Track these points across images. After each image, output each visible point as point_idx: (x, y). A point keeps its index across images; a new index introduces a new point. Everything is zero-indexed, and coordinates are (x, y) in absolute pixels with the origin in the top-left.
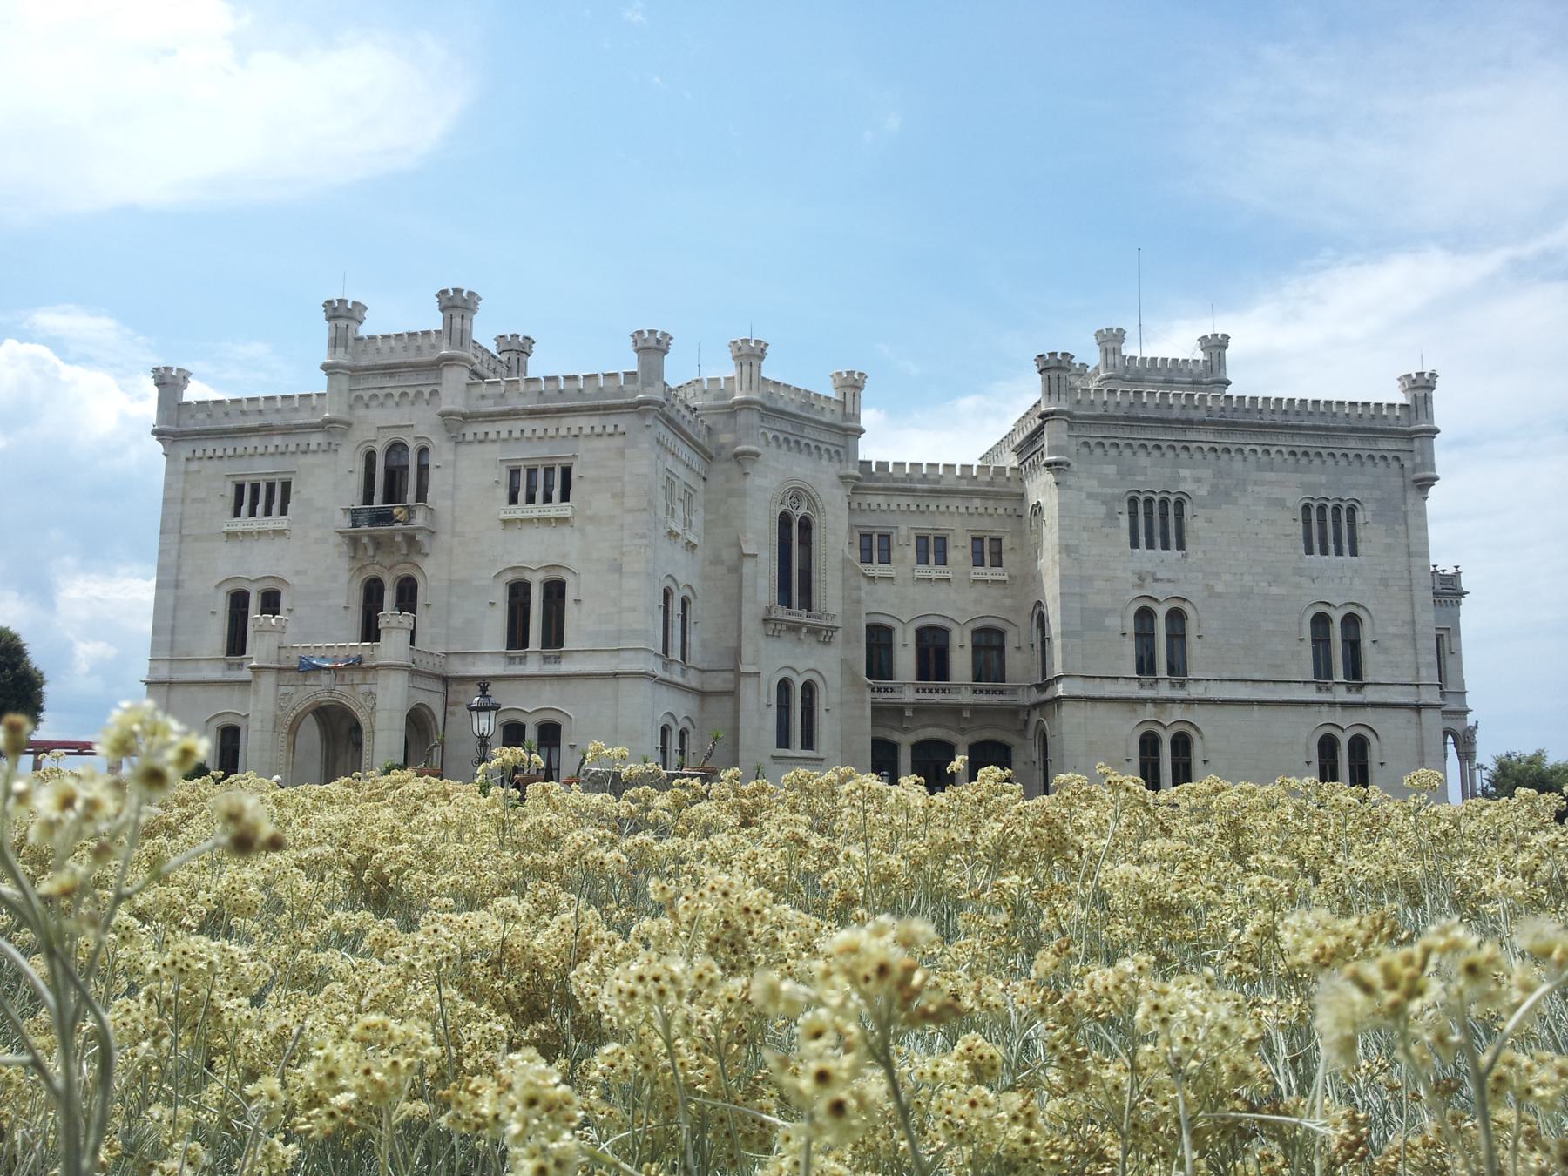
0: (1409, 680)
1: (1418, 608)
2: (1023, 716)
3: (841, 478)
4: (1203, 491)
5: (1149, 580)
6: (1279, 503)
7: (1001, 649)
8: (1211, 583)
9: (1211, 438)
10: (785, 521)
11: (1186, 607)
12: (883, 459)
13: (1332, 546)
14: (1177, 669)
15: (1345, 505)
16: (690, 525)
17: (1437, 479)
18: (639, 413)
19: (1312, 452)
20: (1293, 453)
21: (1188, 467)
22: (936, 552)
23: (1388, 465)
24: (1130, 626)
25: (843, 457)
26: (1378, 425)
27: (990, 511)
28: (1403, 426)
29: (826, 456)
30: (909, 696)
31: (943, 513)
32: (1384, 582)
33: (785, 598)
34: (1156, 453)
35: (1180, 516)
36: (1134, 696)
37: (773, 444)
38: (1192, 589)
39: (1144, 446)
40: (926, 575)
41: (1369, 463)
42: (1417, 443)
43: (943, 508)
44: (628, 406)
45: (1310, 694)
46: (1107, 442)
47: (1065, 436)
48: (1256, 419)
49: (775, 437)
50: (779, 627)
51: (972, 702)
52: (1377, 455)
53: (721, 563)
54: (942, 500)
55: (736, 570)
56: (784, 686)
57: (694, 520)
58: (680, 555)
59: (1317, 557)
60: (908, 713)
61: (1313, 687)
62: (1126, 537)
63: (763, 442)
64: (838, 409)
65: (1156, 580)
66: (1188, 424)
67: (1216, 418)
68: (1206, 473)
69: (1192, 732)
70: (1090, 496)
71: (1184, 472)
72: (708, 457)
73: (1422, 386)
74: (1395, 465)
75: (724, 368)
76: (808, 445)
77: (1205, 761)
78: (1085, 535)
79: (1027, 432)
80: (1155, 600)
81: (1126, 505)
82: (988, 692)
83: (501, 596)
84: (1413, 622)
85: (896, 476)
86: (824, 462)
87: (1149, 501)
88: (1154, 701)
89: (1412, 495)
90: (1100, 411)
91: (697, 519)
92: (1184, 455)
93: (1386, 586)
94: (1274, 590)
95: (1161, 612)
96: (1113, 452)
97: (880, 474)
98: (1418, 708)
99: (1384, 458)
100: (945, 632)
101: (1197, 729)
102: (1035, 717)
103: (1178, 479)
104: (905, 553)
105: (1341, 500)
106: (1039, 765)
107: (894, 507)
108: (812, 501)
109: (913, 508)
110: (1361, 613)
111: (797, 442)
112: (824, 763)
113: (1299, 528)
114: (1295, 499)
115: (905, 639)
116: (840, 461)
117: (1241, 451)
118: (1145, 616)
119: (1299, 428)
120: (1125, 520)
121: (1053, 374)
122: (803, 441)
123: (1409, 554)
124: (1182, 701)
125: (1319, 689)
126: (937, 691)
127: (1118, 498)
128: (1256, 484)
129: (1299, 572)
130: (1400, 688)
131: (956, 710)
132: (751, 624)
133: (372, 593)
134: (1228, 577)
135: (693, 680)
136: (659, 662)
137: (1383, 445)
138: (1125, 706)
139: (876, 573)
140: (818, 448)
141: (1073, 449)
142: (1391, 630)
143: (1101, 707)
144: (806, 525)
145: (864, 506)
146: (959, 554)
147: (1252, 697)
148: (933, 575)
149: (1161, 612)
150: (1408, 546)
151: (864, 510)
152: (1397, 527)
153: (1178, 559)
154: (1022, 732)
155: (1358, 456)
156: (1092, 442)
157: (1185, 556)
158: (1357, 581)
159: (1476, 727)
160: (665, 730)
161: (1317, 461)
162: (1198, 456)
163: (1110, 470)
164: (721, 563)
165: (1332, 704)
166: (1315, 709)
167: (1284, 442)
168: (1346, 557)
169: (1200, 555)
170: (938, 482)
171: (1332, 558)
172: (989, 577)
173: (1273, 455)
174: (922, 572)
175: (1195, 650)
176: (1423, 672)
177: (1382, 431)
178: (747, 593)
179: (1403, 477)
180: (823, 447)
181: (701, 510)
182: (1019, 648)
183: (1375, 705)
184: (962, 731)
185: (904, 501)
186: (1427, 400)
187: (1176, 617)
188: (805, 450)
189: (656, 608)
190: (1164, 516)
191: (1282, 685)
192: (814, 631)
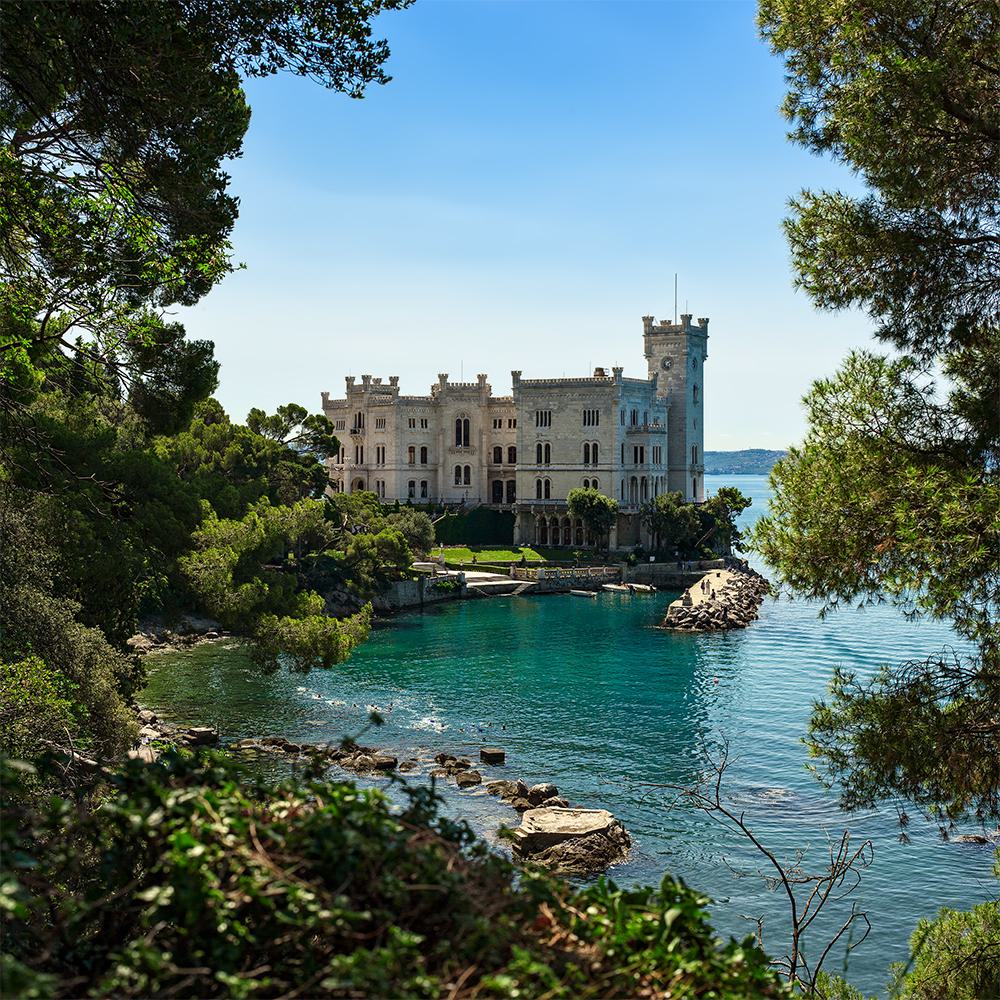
10: (459, 421)
14: (548, 461)
24: (535, 449)
32: (605, 433)
45: (582, 467)
56: (458, 469)
62: (535, 423)
83: (376, 450)
98: (611, 471)
114: (581, 409)
118: (539, 446)
120: (535, 418)
129: (580, 431)
133: (357, 447)
135: (429, 467)
144: (467, 422)
163: (531, 404)
187: (548, 447)
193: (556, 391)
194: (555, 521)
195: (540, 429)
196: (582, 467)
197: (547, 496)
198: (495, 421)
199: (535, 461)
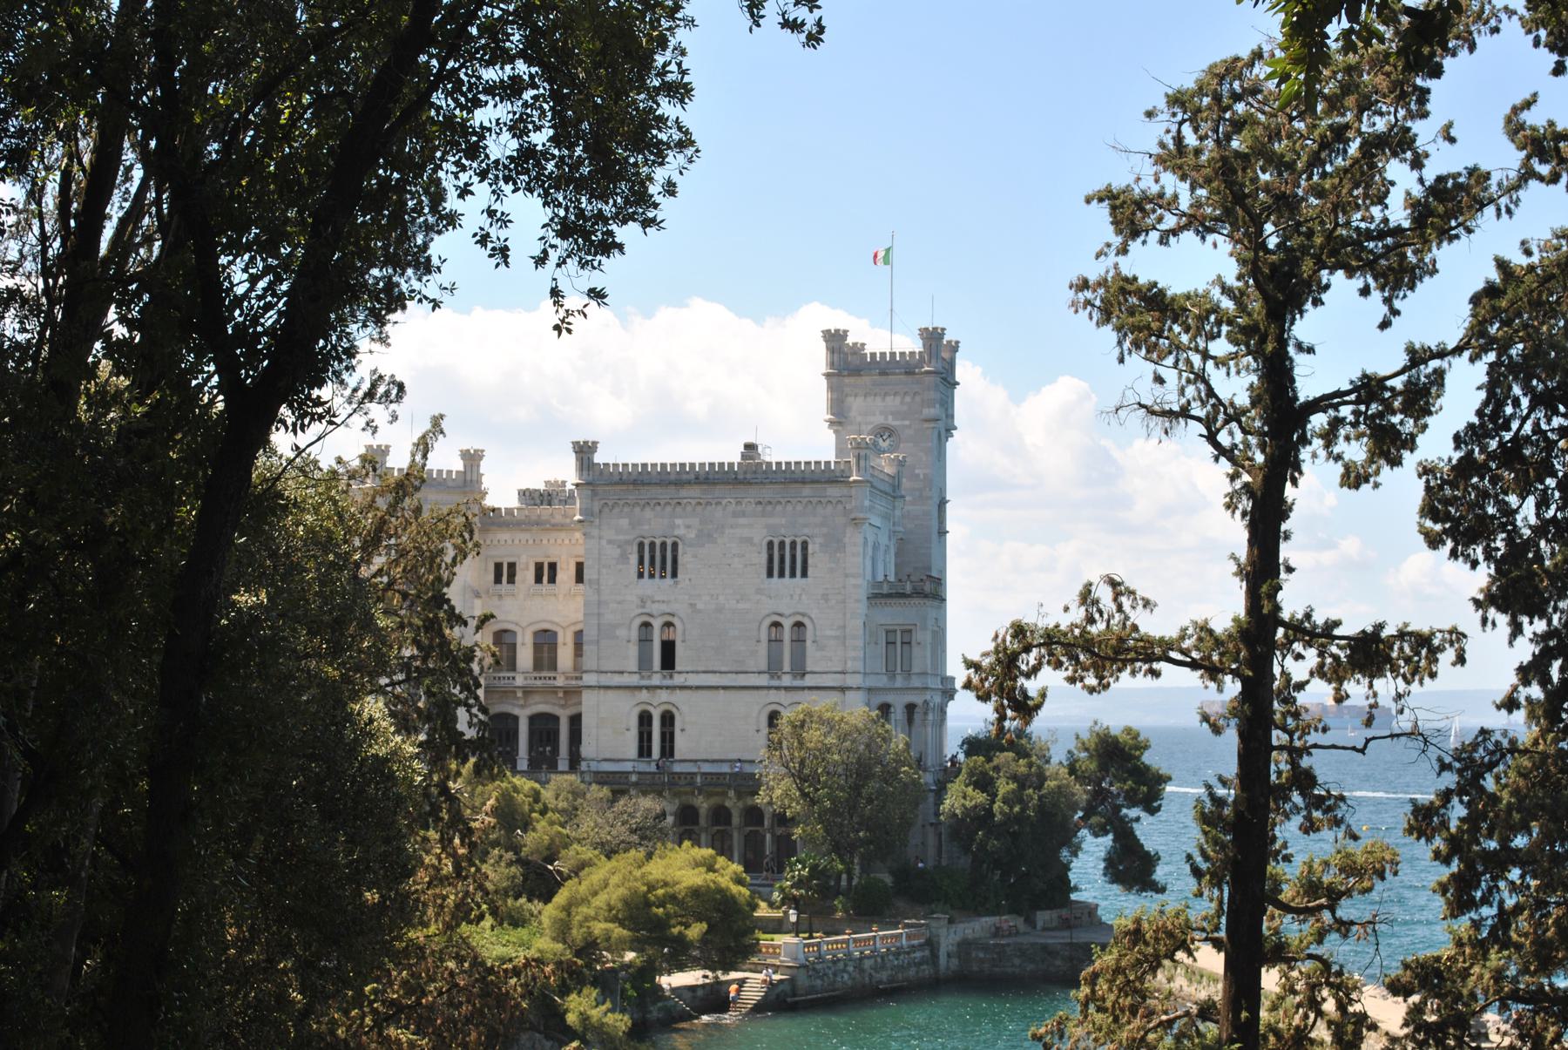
0: (840, 669)
1: (848, 616)
4: (693, 536)
6: (749, 541)
11: (676, 621)
14: (668, 661)
19: (773, 501)
20: (760, 503)
21: (681, 517)
24: (634, 634)
32: (825, 597)
34: (658, 508)
38: (680, 608)
45: (763, 680)
60: (520, 694)
68: (695, 522)
69: (674, 710)
70: (610, 542)
71: (678, 521)
77: (682, 730)
81: (635, 548)
87: (652, 545)
88: (647, 688)
90: (617, 478)
93: (827, 600)
94: (740, 606)
97: (508, 518)
98: (843, 689)
100: (555, 633)
103: (673, 526)
104: (526, 575)
107: (517, 542)
109: (531, 542)
110: (806, 621)
114: (760, 536)
120: (634, 559)
124: (667, 688)
125: (772, 677)
127: (628, 543)
128: (732, 527)
129: (759, 591)
131: (554, 690)
141: (596, 509)
142: (829, 633)
143: (610, 693)
158: (804, 597)
165: (777, 688)
166: (765, 692)
171: (787, 580)
176: (850, 664)
183: (810, 688)
184: (563, 706)
193: (695, 492)
196: (763, 680)
198: (498, 567)
199: (633, 665)
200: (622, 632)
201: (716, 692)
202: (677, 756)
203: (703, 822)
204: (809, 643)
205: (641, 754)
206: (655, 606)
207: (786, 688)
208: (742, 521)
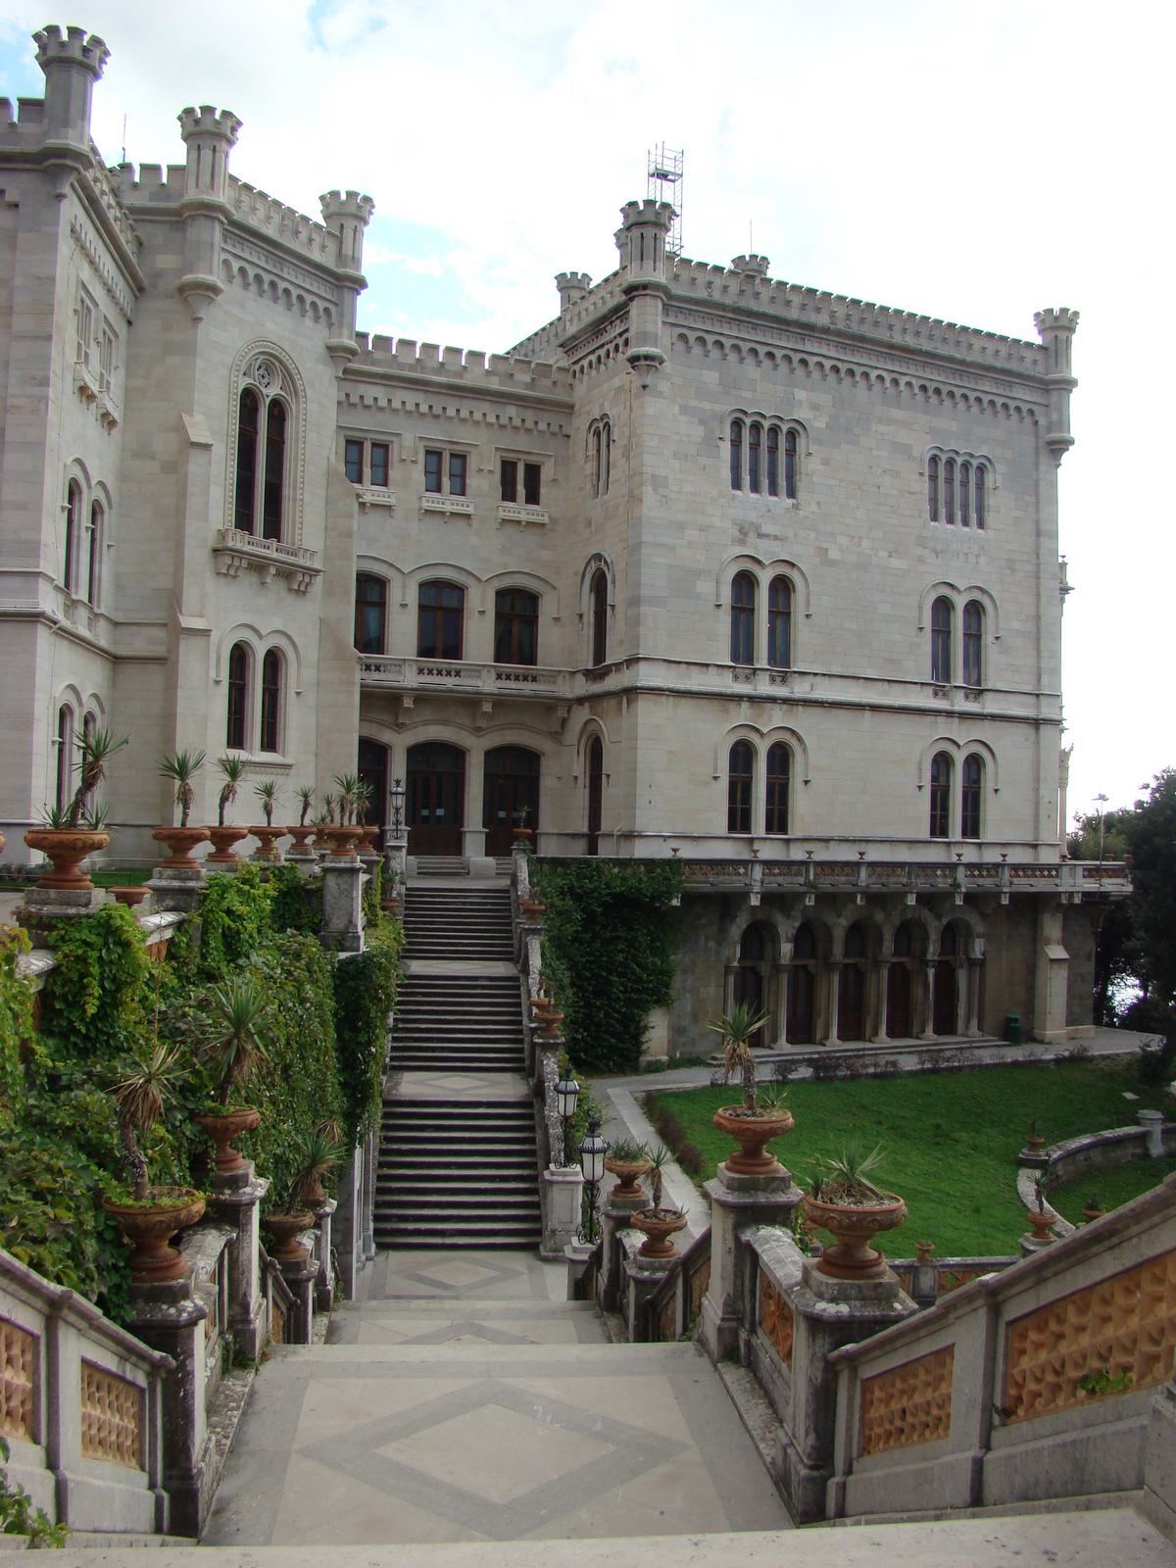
0: (1029, 688)
1: (1044, 600)
2: (561, 713)
3: (330, 349)
5: (752, 535)
6: (902, 450)
7: (531, 621)
8: (824, 546)
9: (833, 354)
10: (249, 401)
11: (795, 576)
12: (385, 334)
13: (958, 515)
14: (781, 654)
15: (975, 463)
16: (108, 388)
17: (1071, 442)
18: (45, 171)
19: (945, 390)
20: (924, 388)
22: (451, 475)
23: (1022, 419)
24: (726, 596)
25: (334, 319)
26: (1014, 366)
27: (529, 424)
28: (1039, 371)
29: (310, 313)
30: (410, 679)
31: (464, 420)
33: (244, 521)
34: (767, 363)
35: (791, 453)
36: (729, 691)
37: (238, 280)
39: (754, 352)
40: (438, 507)
41: (1002, 414)
42: (1054, 397)
43: (464, 414)
44: (24, 158)
45: (925, 700)
46: (710, 339)
47: (660, 322)
48: (882, 335)
49: (242, 270)
50: (237, 563)
51: (496, 691)
52: (1012, 404)
53: (152, 456)
54: (466, 402)
55: (174, 468)
56: (239, 656)
57: (112, 381)
58: (94, 430)
59: (942, 526)
60: (408, 703)
61: (930, 690)
62: (726, 473)
63: (223, 273)
64: (332, 246)
65: (761, 536)
66: (807, 329)
67: (841, 326)
68: (825, 399)
69: (793, 742)
71: (801, 395)
72: (139, 289)
73: (1058, 325)
74: (1028, 420)
75: (172, 152)
76: (287, 292)
77: (806, 782)
78: (676, 464)
79: (587, 319)
80: (759, 562)
82: (517, 678)
84: (1038, 618)
85: (400, 360)
86: (308, 322)
88: (753, 699)
89: (1044, 459)
91: (117, 380)
92: (800, 371)
93: (1013, 570)
95: (765, 578)
96: (715, 353)
97: (379, 355)
98: (1036, 723)
99: (1018, 409)
100: (459, 590)
101: (799, 739)
102: (581, 715)
105: (972, 456)
106: (584, 781)
108: (289, 378)
109: (424, 409)
111: (273, 284)
112: (293, 772)
113: (924, 486)
114: (923, 448)
115: (404, 598)
116: (330, 325)
117: (866, 375)
118: (744, 582)
119: (934, 356)
120: (726, 448)
121: (649, 232)
122: (282, 285)
123: (1038, 534)
124: (786, 701)
125: (936, 694)
126: (449, 673)
129: (921, 541)
130: (1021, 697)
131: (470, 702)
132: (197, 556)
134: (843, 540)
135: (102, 637)
136: (61, 598)
137: (1020, 393)
138: (716, 704)
139: (368, 498)
140: (300, 298)
142: (1016, 625)
143: (684, 702)
144: (278, 411)
145: (355, 399)
146: (484, 481)
147: (865, 700)
148: (448, 508)
149: (765, 578)
150: (1037, 522)
151: (354, 405)
152: (1027, 498)
153: (787, 510)
154: (557, 736)
155: (992, 403)
156: (692, 336)
157: (796, 507)
158: (982, 560)
159: (1072, 749)
160: (65, 713)
161: (948, 403)
162: (816, 374)
164: (152, 456)
165: (949, 714)
166: (930, 719)
167: (913, 373)
168: (973, 530)
169: (814, 507)
170: (460, 374)
171: (958, 528)
172: (523, 517)
173: (902, 387)
174: (433, 501)
175: (804, 636)
176: (1045, 680)
177: (1019, 376)
178: (193, 503)
179: (1037, 436)
180: (309, 299)
181: (122, 371)
182: (557, 620)
183: (994, 717)
184: (478, 731)
185: (411, 398)
186: (1068, 342)
187: (782, 587)
188: (283, 300)
189: (59, 509)
190: (773, 450)
191: (897, 686)
192: (286, 573)
194: (809, 937)
195: (751, 503)
197: (778, 820)
200: (705, 587)
201: (857, 713)
202: (796, 829)
203: (838, 950)
204: (988, 639)
205: (732, 827)
206: (764, 544)
207: (964, 716)
208: (897, 413)
